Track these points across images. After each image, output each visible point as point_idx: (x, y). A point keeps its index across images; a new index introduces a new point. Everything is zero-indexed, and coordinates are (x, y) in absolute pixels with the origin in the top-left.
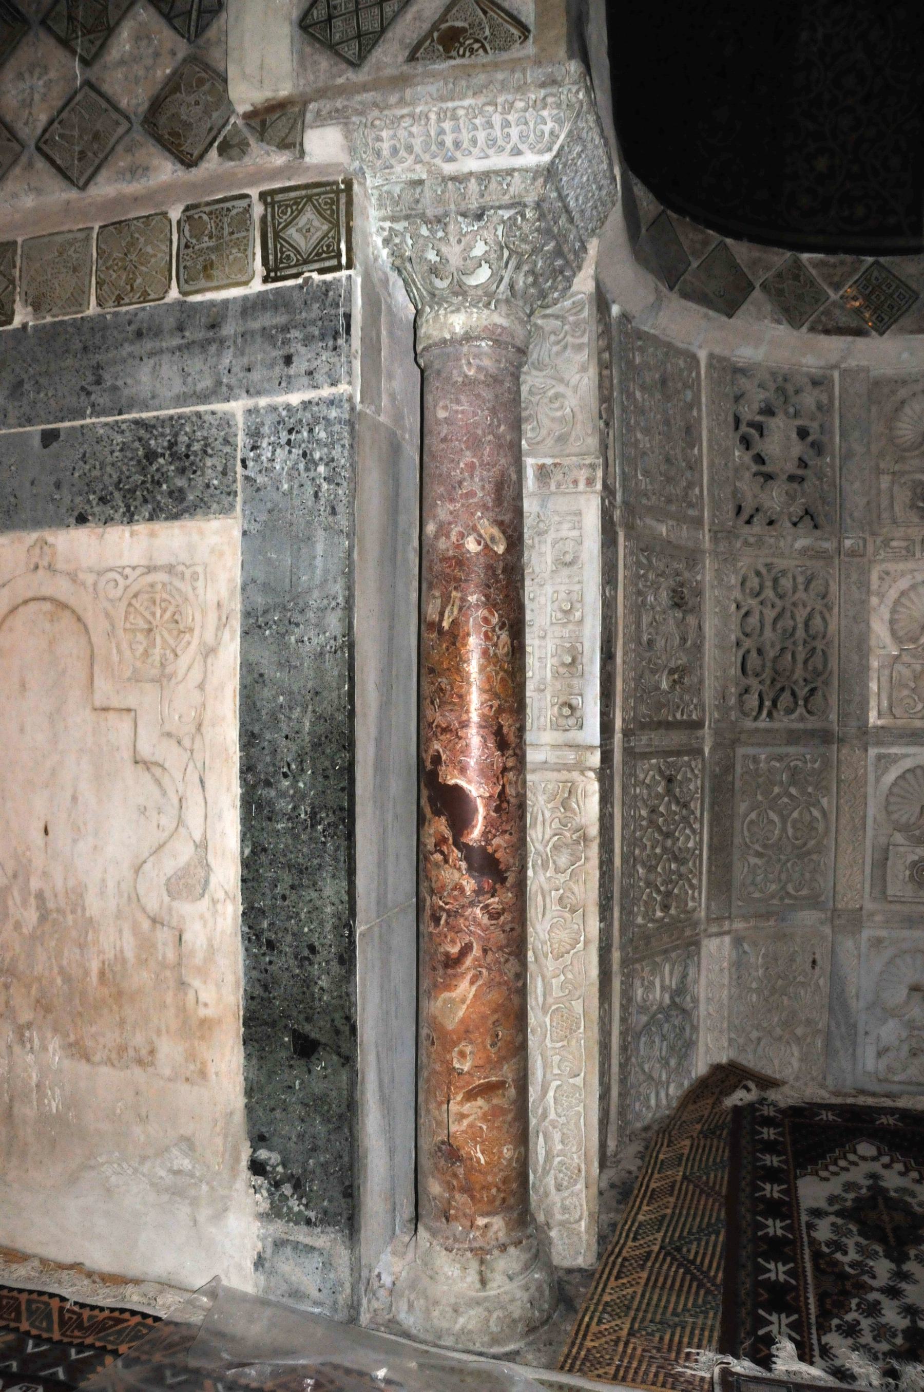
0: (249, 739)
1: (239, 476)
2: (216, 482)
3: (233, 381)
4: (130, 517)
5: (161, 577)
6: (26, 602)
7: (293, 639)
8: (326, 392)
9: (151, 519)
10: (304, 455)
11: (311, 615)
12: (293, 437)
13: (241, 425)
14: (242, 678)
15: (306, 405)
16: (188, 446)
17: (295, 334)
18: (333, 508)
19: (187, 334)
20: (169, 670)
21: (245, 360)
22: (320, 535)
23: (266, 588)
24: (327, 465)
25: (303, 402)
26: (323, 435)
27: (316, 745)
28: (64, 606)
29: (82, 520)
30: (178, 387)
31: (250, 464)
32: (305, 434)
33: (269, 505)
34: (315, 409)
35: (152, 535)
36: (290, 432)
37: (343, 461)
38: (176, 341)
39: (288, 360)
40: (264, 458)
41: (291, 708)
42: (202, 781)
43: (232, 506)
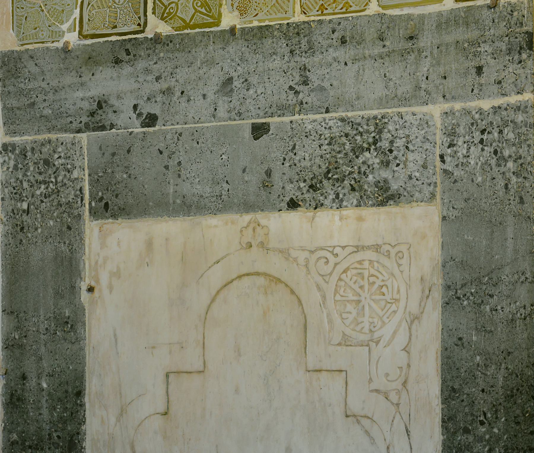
0: (450, 393)
1: (438, 169)
2: (417, 174)
3: (431, 88)
4: (339, 202)
5: (369, 255)
6: (240, 277)
7: (488, 308)
8: (514, 99)
9: (358, 205)
10: (496, 152)
11: (502, 287)
12: (485, 137)
13: (439, 125)
14: (443, 341)
15: (496, 110)
16: (392, 142)
17: (485, 47)
18: (521, 198)
19: (387, 43)
20: (376, 335)
21: (441, 70)
22: (510, 220)
23: (463, 265)
24: (515, 161)
25: (493, 107)
26: (511, 136)
27: (510, 397)
28: (279, 281)
29: (293, 205)
30: (380, 91)
31: (448, 159)
32: (496, 135)
33: (465, 195)
34: (504, 113)
35: (360, 219)
36: (483, 132)
37: (529, 159)
38: (377, 50)
39: (479, 70)
40: (460, 154)
41: (486, 366)
42: (407, 431)
43: (433, 196)
